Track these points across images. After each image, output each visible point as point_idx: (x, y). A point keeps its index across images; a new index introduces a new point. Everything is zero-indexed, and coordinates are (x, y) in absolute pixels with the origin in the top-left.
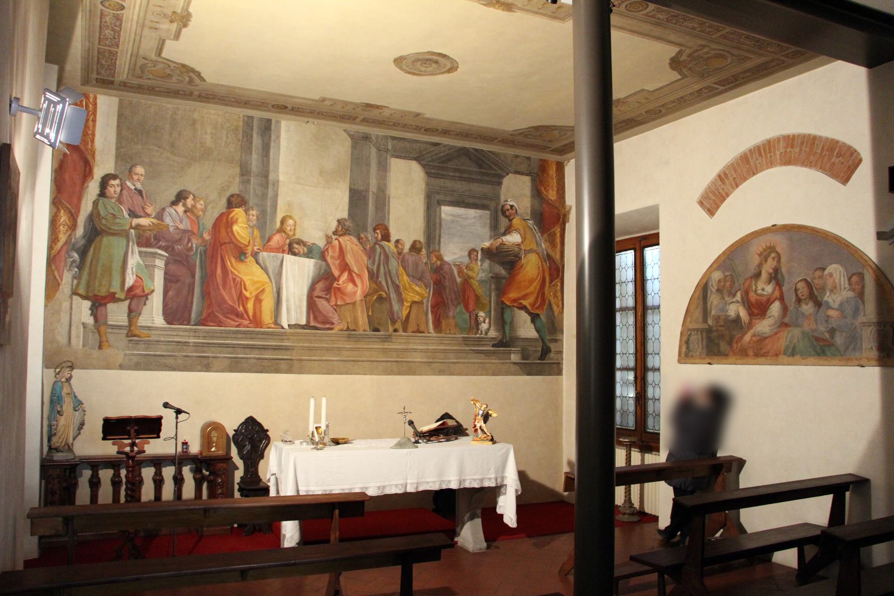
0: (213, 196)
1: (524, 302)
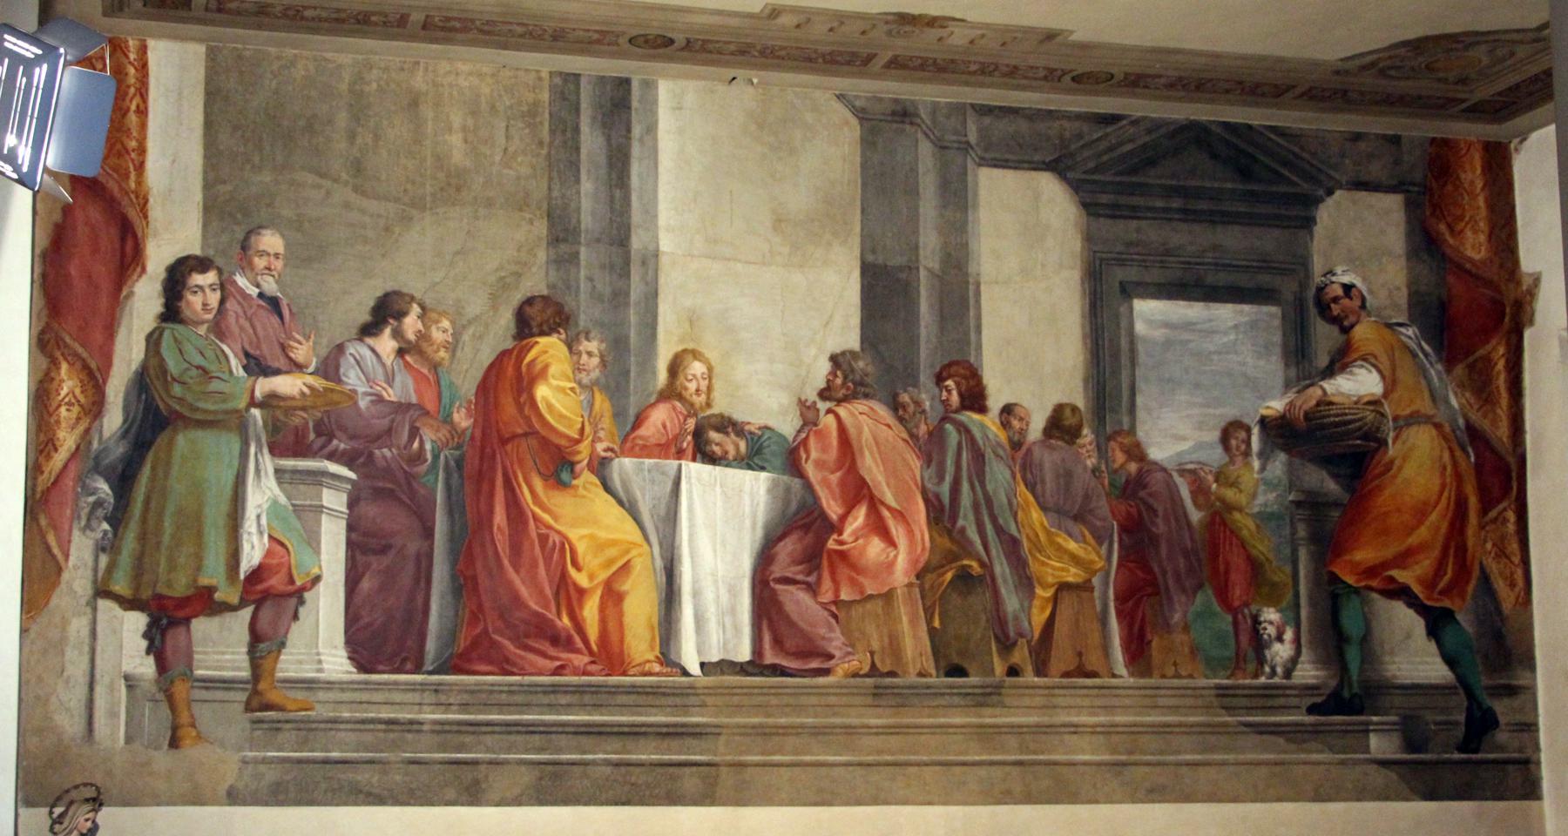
0: (476, 305)
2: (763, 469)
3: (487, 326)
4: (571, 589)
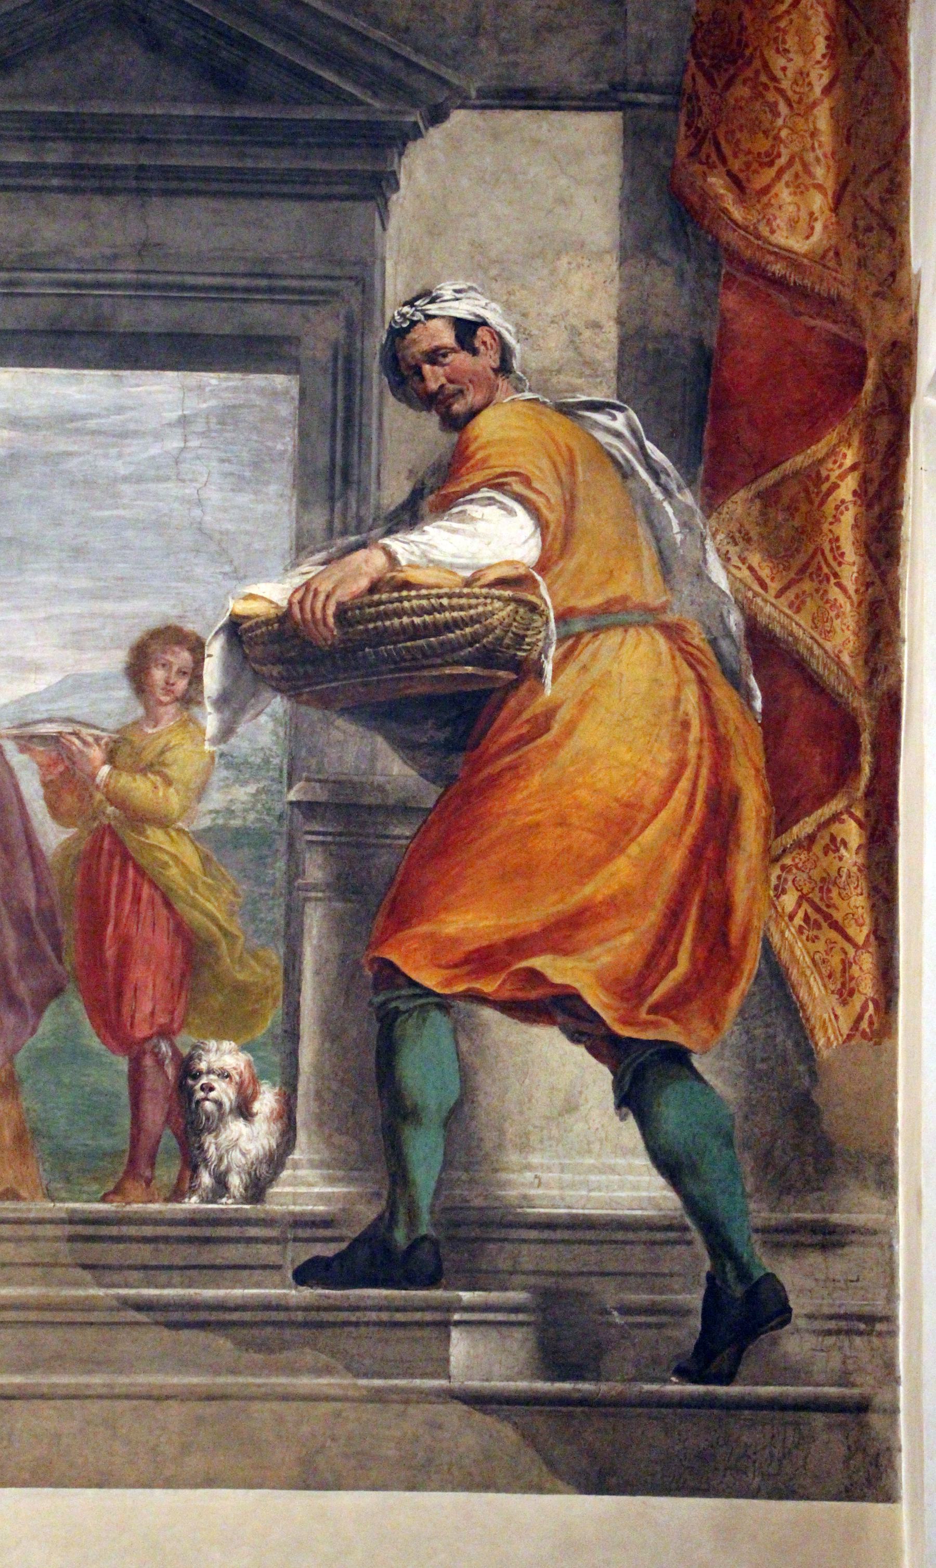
1: (558, 970)
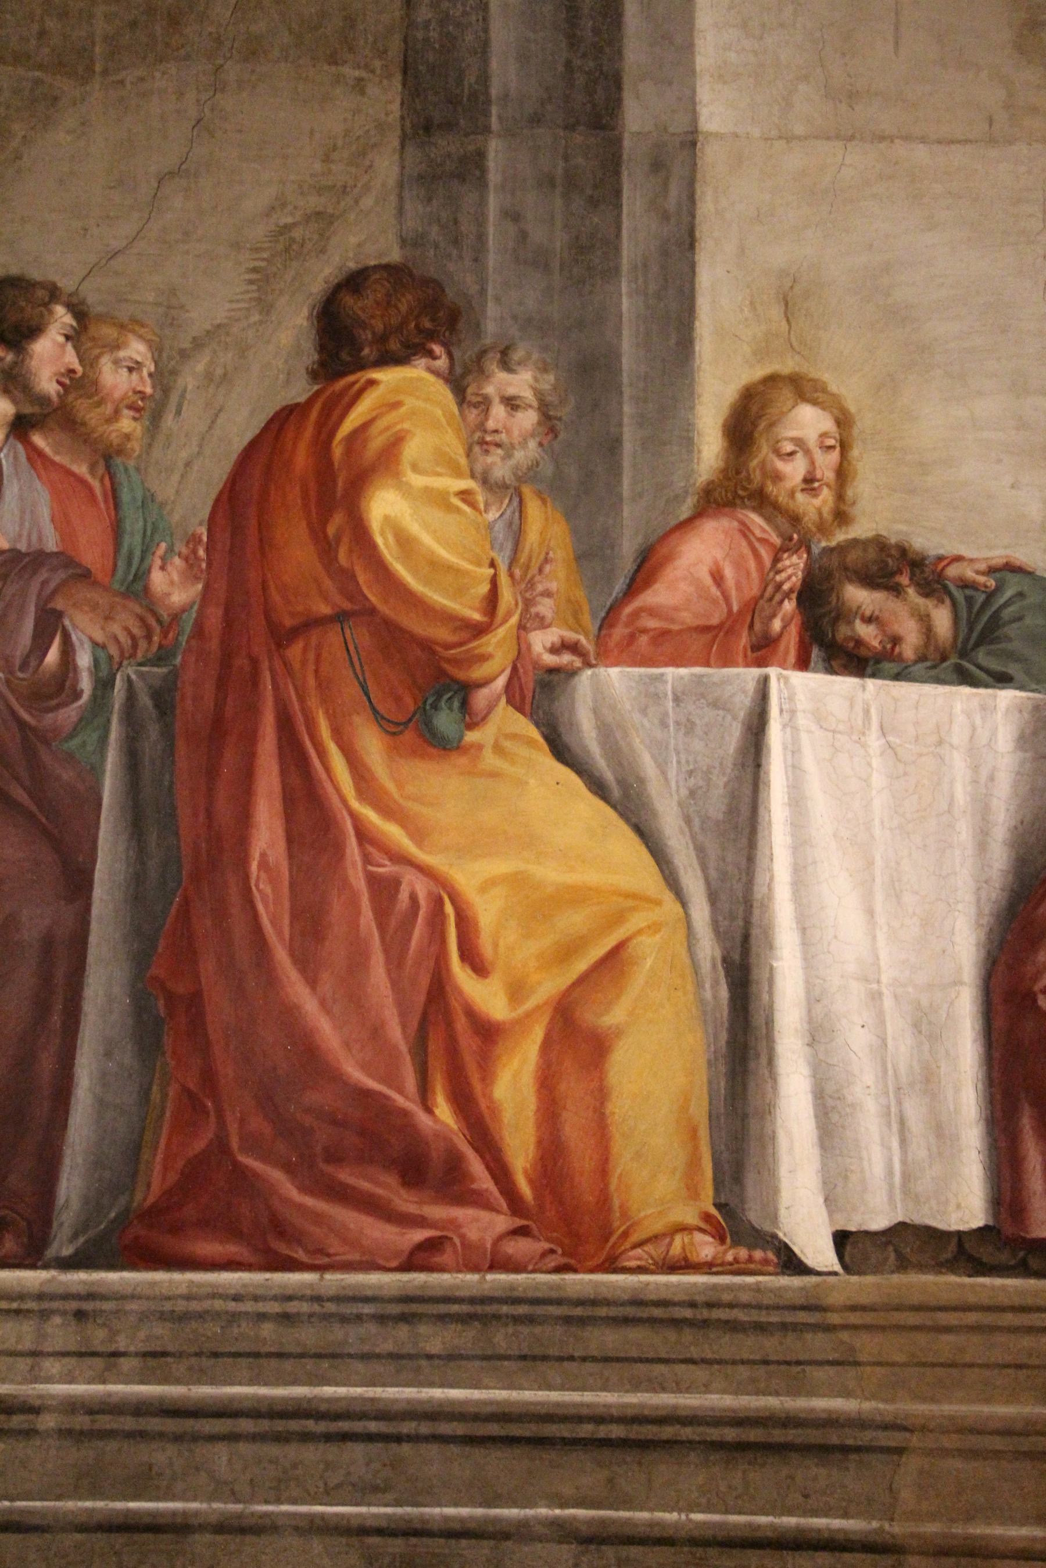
0: (216, 298)
2: (1003, 680)
3: (243, 350)
4: (461, 1024)
